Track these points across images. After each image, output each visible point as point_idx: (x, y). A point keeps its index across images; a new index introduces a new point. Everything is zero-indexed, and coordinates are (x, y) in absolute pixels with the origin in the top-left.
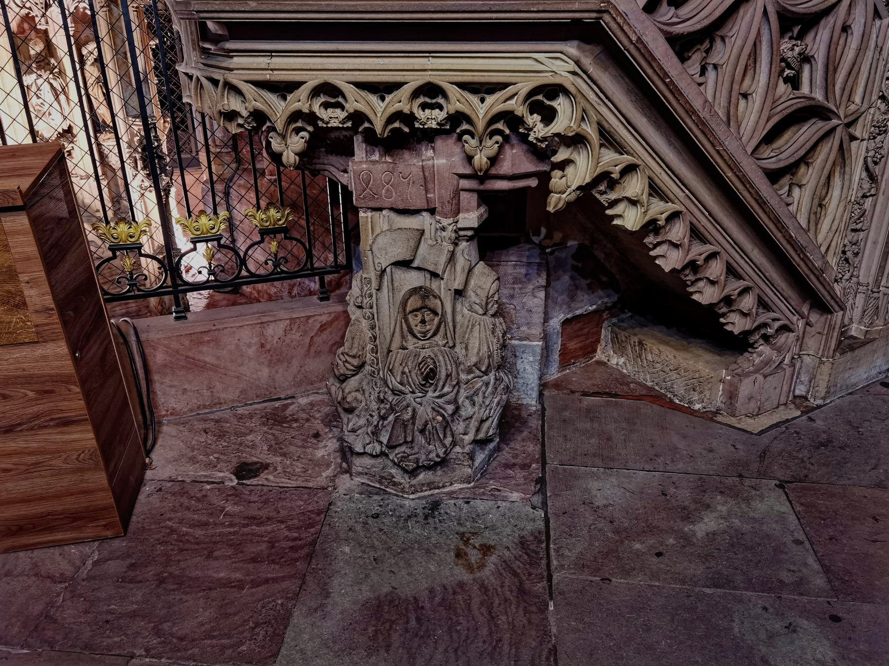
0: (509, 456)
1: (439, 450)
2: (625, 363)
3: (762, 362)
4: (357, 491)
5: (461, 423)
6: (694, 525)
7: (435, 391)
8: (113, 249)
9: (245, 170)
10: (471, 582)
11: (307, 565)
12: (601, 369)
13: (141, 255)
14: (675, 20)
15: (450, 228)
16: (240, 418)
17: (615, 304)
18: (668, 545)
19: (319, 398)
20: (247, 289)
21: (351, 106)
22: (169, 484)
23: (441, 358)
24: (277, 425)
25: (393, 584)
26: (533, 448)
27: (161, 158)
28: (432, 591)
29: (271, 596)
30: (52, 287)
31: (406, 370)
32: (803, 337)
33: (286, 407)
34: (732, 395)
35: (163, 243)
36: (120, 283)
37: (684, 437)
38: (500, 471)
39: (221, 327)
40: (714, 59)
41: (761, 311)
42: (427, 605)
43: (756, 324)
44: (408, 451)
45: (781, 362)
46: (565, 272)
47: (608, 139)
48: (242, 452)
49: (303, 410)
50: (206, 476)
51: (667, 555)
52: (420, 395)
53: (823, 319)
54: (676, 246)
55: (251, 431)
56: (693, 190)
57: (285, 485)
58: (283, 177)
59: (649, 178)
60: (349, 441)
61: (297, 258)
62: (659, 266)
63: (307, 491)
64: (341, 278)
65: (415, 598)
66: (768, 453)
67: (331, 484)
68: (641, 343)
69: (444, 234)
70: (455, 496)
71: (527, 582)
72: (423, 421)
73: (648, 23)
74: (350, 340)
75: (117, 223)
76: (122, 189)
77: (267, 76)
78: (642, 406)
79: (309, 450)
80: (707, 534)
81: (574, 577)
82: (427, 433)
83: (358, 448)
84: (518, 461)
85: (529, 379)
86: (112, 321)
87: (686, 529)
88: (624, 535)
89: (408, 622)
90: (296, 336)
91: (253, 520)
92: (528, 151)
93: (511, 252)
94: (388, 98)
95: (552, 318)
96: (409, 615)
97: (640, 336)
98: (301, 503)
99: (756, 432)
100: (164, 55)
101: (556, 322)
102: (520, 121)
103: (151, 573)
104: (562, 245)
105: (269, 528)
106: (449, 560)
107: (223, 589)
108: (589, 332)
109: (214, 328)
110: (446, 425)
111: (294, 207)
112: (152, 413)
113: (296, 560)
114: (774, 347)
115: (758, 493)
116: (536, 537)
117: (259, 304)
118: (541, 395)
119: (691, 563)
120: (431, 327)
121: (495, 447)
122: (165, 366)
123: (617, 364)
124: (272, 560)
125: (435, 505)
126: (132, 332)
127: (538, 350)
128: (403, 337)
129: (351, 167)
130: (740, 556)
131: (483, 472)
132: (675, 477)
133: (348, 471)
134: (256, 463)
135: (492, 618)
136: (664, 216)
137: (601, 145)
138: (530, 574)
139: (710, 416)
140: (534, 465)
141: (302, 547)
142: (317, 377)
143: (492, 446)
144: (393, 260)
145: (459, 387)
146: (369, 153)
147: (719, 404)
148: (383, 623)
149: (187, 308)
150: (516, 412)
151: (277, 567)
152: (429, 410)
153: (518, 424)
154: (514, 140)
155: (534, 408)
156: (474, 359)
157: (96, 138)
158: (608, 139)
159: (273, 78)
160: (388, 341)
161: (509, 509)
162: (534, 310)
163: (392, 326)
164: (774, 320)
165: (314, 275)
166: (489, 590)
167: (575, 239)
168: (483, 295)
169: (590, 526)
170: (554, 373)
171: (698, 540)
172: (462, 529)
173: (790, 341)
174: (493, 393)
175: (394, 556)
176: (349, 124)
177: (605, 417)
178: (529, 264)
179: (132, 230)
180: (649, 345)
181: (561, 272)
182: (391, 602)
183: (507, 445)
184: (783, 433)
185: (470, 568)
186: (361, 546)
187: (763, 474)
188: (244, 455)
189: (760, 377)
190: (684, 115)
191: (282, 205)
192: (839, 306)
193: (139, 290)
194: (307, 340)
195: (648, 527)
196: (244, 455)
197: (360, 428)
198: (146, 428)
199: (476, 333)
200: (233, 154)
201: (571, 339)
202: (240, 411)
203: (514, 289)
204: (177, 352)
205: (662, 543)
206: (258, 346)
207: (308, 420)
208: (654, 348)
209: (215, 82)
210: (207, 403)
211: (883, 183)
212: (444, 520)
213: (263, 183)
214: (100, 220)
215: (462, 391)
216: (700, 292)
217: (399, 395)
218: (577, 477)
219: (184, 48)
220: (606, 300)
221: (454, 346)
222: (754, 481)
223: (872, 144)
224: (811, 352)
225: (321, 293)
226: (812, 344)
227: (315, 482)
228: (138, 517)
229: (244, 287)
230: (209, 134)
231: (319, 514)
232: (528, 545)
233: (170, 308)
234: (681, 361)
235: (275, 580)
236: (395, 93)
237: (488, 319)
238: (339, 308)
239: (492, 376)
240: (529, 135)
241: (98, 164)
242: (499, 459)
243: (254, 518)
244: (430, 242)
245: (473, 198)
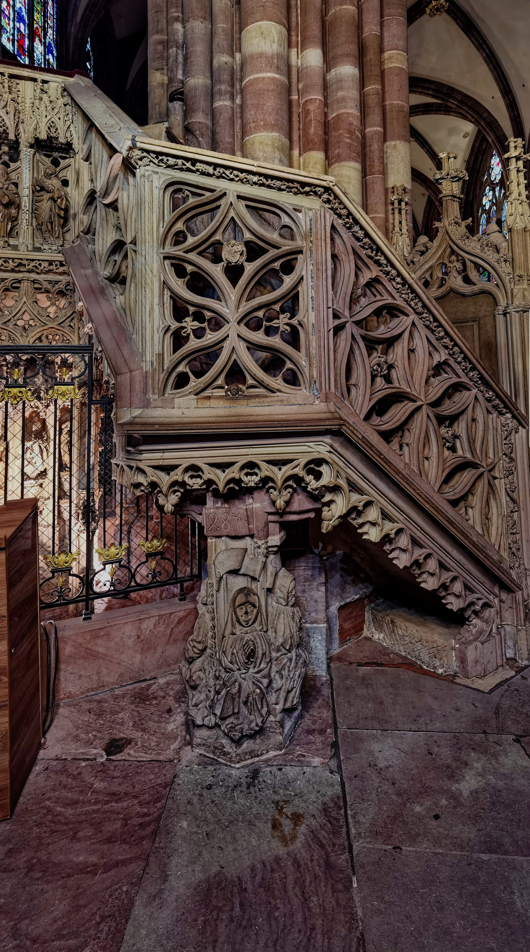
0: (309, 722)
1: (258, 720)
2: (383, 638)
3: (477, 632)
4: (196, 762)
5: (273, 694)
6: (459, 784)
7: (255, 667)
8: (53, 572)
9: (142, 517)
10: (285, 856)
11: (151, 844)
12: (368, 643)
13: (70, 575)
14: (381, 423)
15: (263, 546)
16: (116, 698)
17: (371, 593)
18: (442, 807)
19: (173, 677)
20: (133, 595)
21: (206, 477)
22: (54, 763)
23: (258, 640)
24: (141, 703)
25: (221, 863)
26: (326, 714)
27: (94, 512)
28: (253, 869)
29: (118, 883)
30: (8, 600)
31: (235, 651)
32: (501, 611)
33: (149, 686)
34: (463, 660)
35: (85, 566)
36: (52, 595)
37: (436, 698)
38: (303, 737)
39: (113, 624)
40: (406, 440)
41: (468, 593)
42: (250, 887)
43: (466, 603)
44: (235, 721)
45: (491, 632)
46: (336, 572)
47: (354, 487)
48: (113, 729)
49: (161, 689)
50: (83, 754)
51: (443, 818)
52: (244, 671)
53: (510, 597)
54: (404, 551)
55: (122, 709)
56: (408, 514)
57: (142, 759)
58: (164, 520)
59: (381, 508)
60: (193, 715)
61: (167, 572)
62: (396, 565)
63: (157, 764)
64: (194, 584)
65: (239, 878)
66: (501, 710)
67: (176, 756)
68: (392, 622)
69: (259, 550)
70: (270, 763)
71: (332, 854)
72: (247, 694)
73: (367, 427)
74: (197, 630)
75: (59, 554)
76: (67, 532)
77: (161, 463)
78: (401, 673)
79: (163, 725)
80: (471, 793)
81: (370, 846)
82: (249, 704)
83: (199, 722)
84: (316, 727)
85: (320, 654)
86: (42, 623)
87: (453, 788)
88: (405, 797)
89: (232, 909)
90: (161, 628)
91: (114, 796)
92: (308, 496)
93: (301, 560)
94: (227, 471)
95: (331, 606)
96: (235, 900)
97: (391, 616)
98: (153, 776)
99: (487, 691)
100: (106, 455)
101: (334, 609)
102: (302, 479)
103: (23, 859)
104: (332, 554)
105: (125, 804)
106: (267, 832)
107: (79, 876)
108: (357, 615)
109: (108, 625)
110: (263, 697)
111: (169, 538)
112: (54, 696)
113: (143, 838)
114: (481, 619)
115: (502, 748)
116: (336, 803)
117: (140, 605)
118: (329, 667)
119: (464, 825)
120: (252, 617)
121: (298, 715)
122: (70, 656)
123: (379, 639)
124: (124, 839)
125: (255, 774)
126: (53, 631)
127: (324, 631)
128: (233, 625)
129: (204, 511)
130: (502, 816)
131: (291, 738)
132: (436, 736)
133: (190, 743)
134: (122, 739)
135: (306, 900)
136: (393, 532)
137: (350, 491)
138: (334, 845)
139: (451, 679)
140: (328, 730)
141: (149, 824)
142: (173, 660)
143: (296, 713)
144: (228, 570)
145: (271, 663)
146: (215, 503)
147: (455, 668)
148: (212, 911)
149: (92, 612)
150: (312, 683)
151: (127, 847)
152: (251, 684)
153: (314, 693)
154: (299, 491)
155: (325, 679)
156: (281, 640)
157: (58, 502)
158: (354, 487)
159: (164, 464)
160: (223, 629)
161: (313, 774)
162: (319, 600)
163: (226, 618)
164: (478, 599)
165: (176, 583)
166: (301, 866)
167: (340, 550)
168: (285, 591)
169: (377, 789)
170: (336, 649)
171: (465, 800)
172: (277, 798)
173: (492, 614)
174: (295, 667)
175: (223, 830)
176: (204, 487)
177: (376, 684)
178: (313, 568)
179: (68, 558)
180: (398, 623)
181: (334, 572)
182: (219, 883)
183: (308, 712)
184: (507, 691)
185: (285, 841)
186: (196, 819)
187: (501, 730)
188: (115, 732)
189: (479, 644)
190: (394, 474)
191: (161, 537)
192: (518, 587)
193: (64, 599)
194: (169, 632)
195: (423, 787)
196: (115, 732)
197: (201, 702)
198: (47, 711)
199: (281, 620)
200: (136, 507)
201: (345, 621)
202: (117, 692)
203: (305, 586)
204: (80, 645)
205: (436, 804)
206: (136, 637)
207: (164, 697)
208: (402, 625)
209: (131, 468)
210: (94, 687)
211: (521, 503)
212: (262, 788)
213: (152, 524)
214: (50, 553)
215: (273, 666)
216: (425, 582)
217: (229, 672)
218: (362, 740)
219: (117, 451)
220: (365, 590)
221: (267, 630)
222: (496, 737)
223: (507, 481)
224: (509, 623)
225: (181, 595)
226: (508, 616)
227: (165, 755)
228: (25, 798)
229: (132, 594)
230: (124, 496)
231: (165, 788)
232: (330, 812)
233: (81, 611)
234: (422, 634)
235: (124, 863)
236: (231, 468)
237: (289, 609)
238: (192, 606)
239: (293, 653)
240: (307, 487)
241: (56, 517)
242: (302, 725)
243: (114, 794)
244: (251, 556)
245: (277, 527)
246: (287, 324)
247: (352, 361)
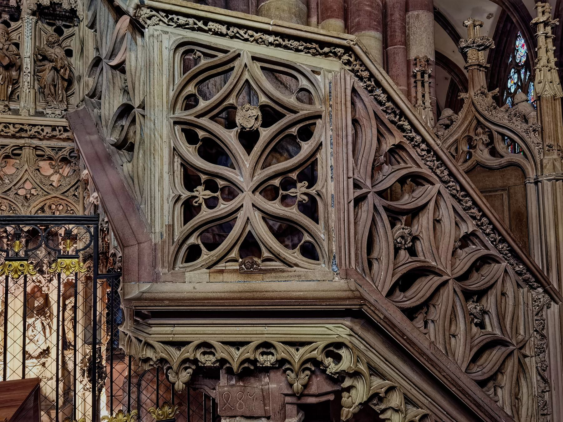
246: (305, 194)
247: (375, 234)
